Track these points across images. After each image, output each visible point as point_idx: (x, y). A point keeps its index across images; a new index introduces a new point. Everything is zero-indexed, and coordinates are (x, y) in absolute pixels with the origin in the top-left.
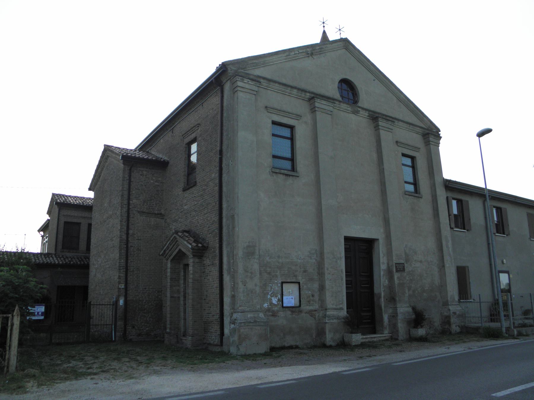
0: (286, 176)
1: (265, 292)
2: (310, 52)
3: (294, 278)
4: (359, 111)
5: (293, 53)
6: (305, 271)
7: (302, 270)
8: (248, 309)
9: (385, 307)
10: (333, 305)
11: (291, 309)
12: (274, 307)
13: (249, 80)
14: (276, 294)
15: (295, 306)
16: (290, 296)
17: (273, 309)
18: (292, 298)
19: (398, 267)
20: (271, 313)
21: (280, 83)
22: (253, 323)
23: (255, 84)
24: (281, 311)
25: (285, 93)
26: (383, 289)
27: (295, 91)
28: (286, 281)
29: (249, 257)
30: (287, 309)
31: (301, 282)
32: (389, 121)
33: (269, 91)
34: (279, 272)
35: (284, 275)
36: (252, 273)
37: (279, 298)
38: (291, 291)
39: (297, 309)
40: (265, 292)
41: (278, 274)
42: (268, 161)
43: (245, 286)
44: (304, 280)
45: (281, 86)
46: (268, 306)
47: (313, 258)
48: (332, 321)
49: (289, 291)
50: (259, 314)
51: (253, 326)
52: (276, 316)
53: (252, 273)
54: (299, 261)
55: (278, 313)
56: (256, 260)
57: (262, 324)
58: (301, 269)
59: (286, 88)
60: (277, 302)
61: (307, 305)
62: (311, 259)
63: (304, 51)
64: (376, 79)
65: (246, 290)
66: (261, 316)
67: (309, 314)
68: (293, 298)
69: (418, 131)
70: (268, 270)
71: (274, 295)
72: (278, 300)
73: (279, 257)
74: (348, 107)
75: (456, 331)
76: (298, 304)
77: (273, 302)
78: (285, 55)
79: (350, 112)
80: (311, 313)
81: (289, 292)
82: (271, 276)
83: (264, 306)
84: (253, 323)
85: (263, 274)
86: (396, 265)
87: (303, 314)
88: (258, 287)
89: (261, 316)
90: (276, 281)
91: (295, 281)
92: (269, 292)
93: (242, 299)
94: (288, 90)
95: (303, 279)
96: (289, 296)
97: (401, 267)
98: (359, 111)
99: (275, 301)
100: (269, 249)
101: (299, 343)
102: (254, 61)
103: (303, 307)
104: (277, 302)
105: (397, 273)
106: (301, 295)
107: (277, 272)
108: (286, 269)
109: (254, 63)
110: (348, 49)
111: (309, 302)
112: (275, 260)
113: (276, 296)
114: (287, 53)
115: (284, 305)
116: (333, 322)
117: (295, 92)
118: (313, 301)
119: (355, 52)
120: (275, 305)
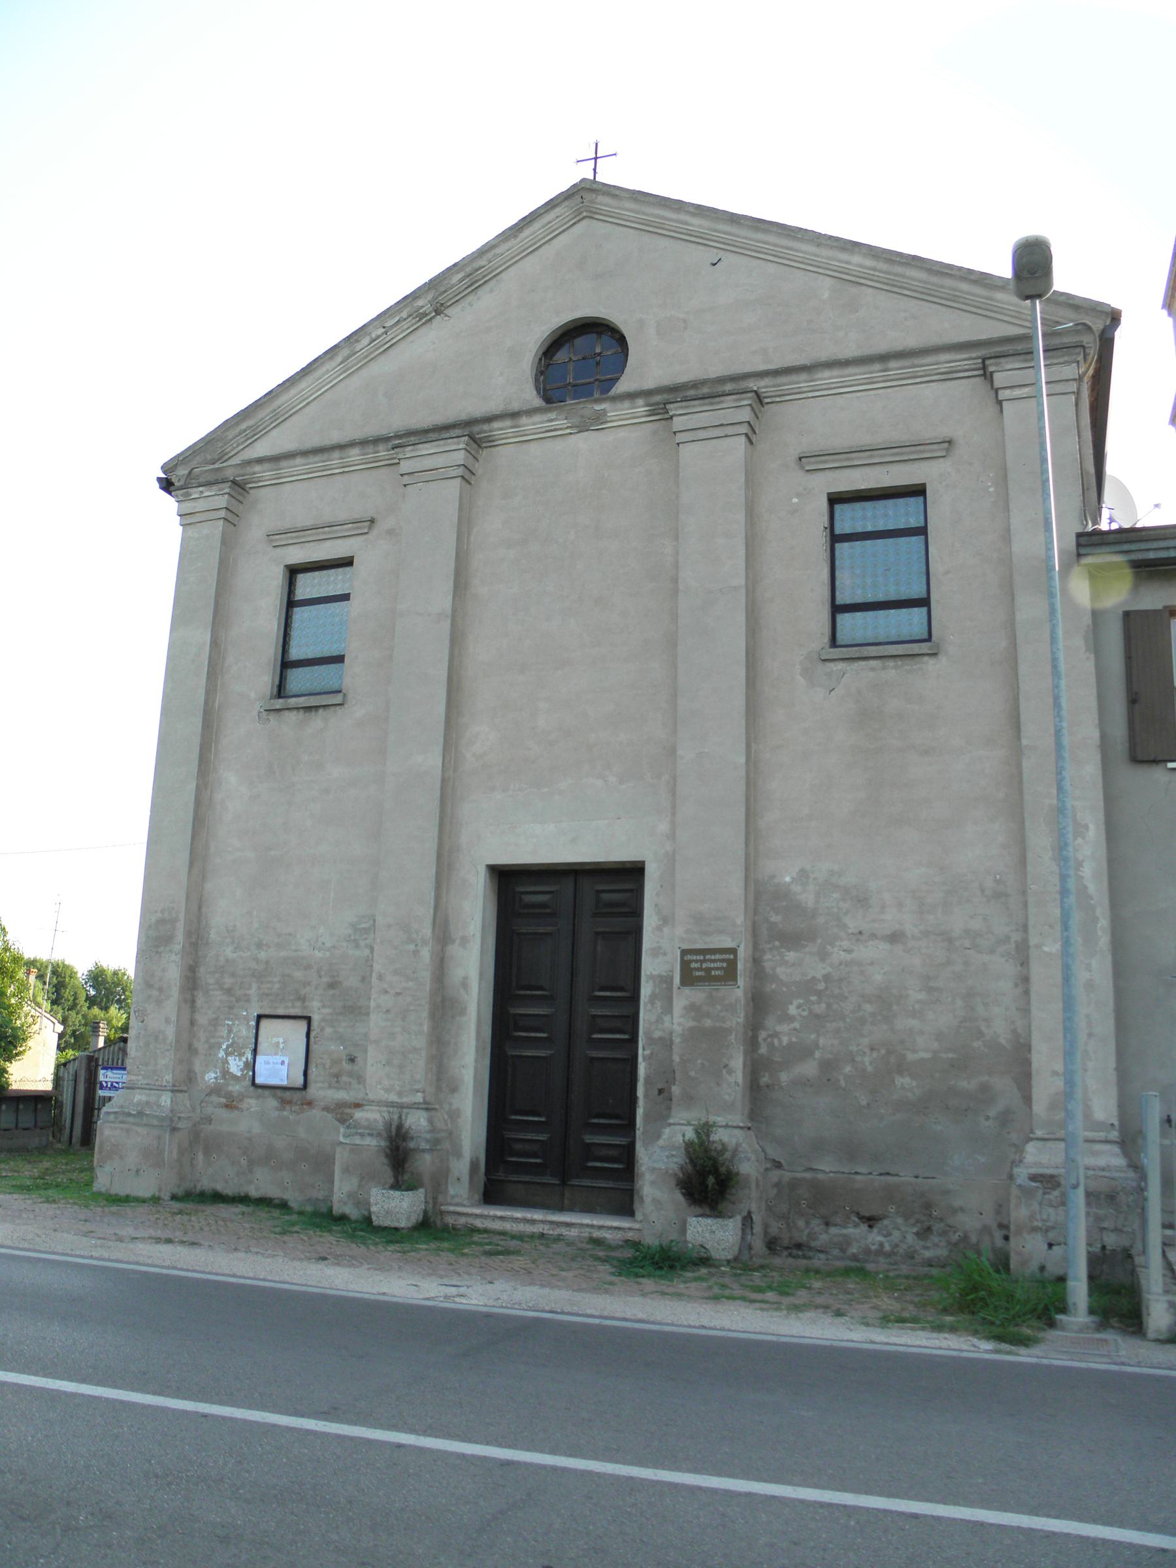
0: (305, 712)
1: (212, 1041)
2: (428, 308)
3: (298, 1004)
4: (604, 411)
5: (366, 341)
6: (332, 985)
7: (325, 980)
8: (146, 1082)
9: (646, 1115)
10: (388, 1090)
11: (279, 1092)
12: (232, 1082)
13: (201, 489)
14: (242, 1048)
15: (289, 1086)
16: (278, 1057)
17: (230, 1088)
18: (283, 1063)
19: (694, 965)
20: (223, 1100)
21: (305, 453)
22: (134, 1116)
23: (220, 490)
24: (252, 1097)
25: (329, 472)
26: (644, 1049)
27: (355, 451)
28: (272, 1013)
29: (159, 950)
30: (267, 1092)
31: (316, 1018)
32: (722, 398)
33: (288, 487)
34: (254, 986)
35: (268, 995)
36: (161, 990)
37: (247, 1059)
38: (281, 1040)
39: (297, 1096)
40: (212, 1041)
41: (253, 991)
42: (353, 675)
43: (143, 1022)
44: (327, 1011)
45: (312, 459)
46: (216, 1078)
47: (362, 943)
48: (357, 1140)
49: (275, 1040)
50: (160, 1096)
51: (134, 1124)
52: (237, 1108)
53: (161, 990)
54: (318, 954)
55: (242, 1100)
56: (173, 957)
57: (155, 1122)
58: (320, 977)
59: (326, 456)
60: (242, 1070)
61: (330, 1087)
62: (357, 946)
63: (404, 314)
64: (721, 254)
65: (142, 1032)
66: (165, 1101)
67: (337, 1114)
68: (286, 1063)
69: (944, 368)
70: (228, 981)
71: (235, 1049)
72: (246, 1064)
73: (259, 945)
74: (551, 420)
75: (1042, 1268)
76: (300, 1081)
77: (231, 1070)
78: (339, 359)
79: (568, 431)
80: (341, 1111)
81: (277, 1044)
82: (234, 999)
83: (206, 1079)
84: (134, 1116)
85: (211, 993)
86: (689, 957)
87: (316, 1113)
88: (172, 1025)
89: (165, 1101)
90: (245, 1014)
91: (300, 1014)
92: (221, 1040)
93: (133, 1056)
94: (335, 459)
95: (324, 1006)
96: (276, 1054)
97: (718, 965)
98: (604, 411)
99: (235, 1066)
100: (235, 926)
101: (293, 1197)
102: (244, 426)
103: (314, 1091)
104: (242, 1070)
105: (687, 991)
106: (311, 1055)
107: (250, 988)
108: (276, 979)
109: (245, 431)
110: (596, 213)
111: (337, 1076)
112: (249, 953)
113: (241, 1055)
114: (345, 352)
115: (258, 1081)
116: (362, 1143)
117: (354, 454)
118: (350, 1075)
119: (622, 209)
120: (235, 1077)
